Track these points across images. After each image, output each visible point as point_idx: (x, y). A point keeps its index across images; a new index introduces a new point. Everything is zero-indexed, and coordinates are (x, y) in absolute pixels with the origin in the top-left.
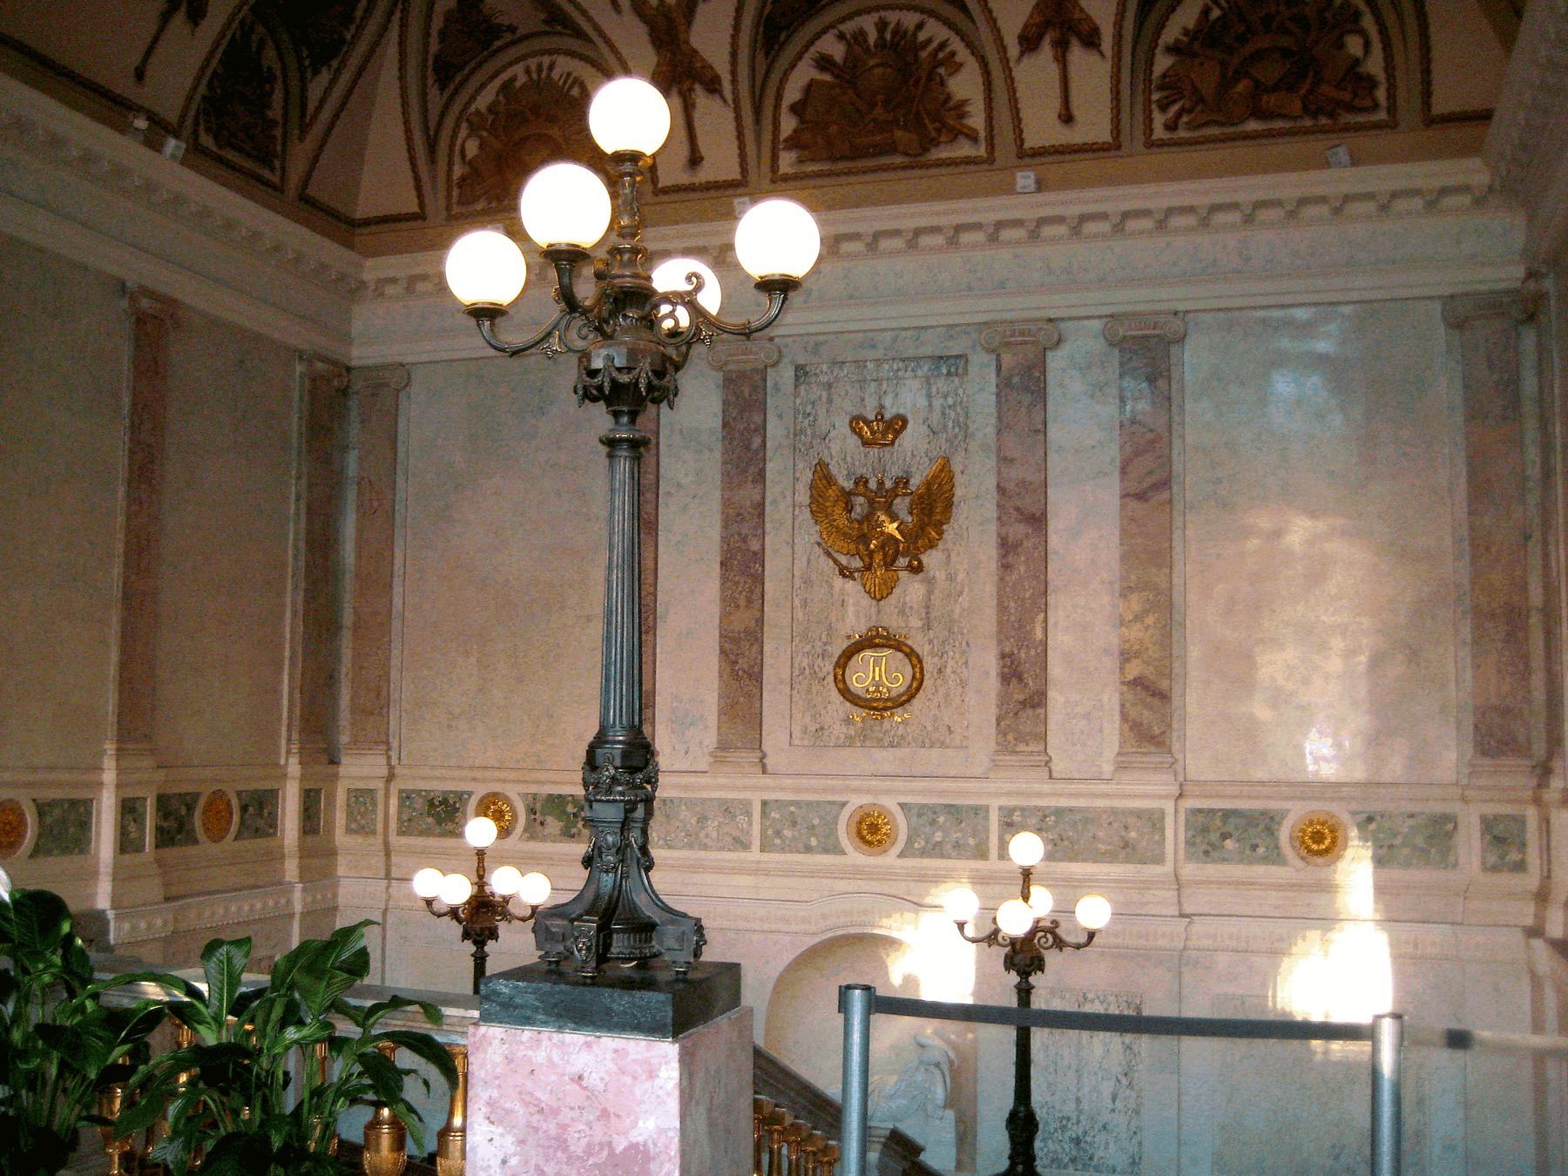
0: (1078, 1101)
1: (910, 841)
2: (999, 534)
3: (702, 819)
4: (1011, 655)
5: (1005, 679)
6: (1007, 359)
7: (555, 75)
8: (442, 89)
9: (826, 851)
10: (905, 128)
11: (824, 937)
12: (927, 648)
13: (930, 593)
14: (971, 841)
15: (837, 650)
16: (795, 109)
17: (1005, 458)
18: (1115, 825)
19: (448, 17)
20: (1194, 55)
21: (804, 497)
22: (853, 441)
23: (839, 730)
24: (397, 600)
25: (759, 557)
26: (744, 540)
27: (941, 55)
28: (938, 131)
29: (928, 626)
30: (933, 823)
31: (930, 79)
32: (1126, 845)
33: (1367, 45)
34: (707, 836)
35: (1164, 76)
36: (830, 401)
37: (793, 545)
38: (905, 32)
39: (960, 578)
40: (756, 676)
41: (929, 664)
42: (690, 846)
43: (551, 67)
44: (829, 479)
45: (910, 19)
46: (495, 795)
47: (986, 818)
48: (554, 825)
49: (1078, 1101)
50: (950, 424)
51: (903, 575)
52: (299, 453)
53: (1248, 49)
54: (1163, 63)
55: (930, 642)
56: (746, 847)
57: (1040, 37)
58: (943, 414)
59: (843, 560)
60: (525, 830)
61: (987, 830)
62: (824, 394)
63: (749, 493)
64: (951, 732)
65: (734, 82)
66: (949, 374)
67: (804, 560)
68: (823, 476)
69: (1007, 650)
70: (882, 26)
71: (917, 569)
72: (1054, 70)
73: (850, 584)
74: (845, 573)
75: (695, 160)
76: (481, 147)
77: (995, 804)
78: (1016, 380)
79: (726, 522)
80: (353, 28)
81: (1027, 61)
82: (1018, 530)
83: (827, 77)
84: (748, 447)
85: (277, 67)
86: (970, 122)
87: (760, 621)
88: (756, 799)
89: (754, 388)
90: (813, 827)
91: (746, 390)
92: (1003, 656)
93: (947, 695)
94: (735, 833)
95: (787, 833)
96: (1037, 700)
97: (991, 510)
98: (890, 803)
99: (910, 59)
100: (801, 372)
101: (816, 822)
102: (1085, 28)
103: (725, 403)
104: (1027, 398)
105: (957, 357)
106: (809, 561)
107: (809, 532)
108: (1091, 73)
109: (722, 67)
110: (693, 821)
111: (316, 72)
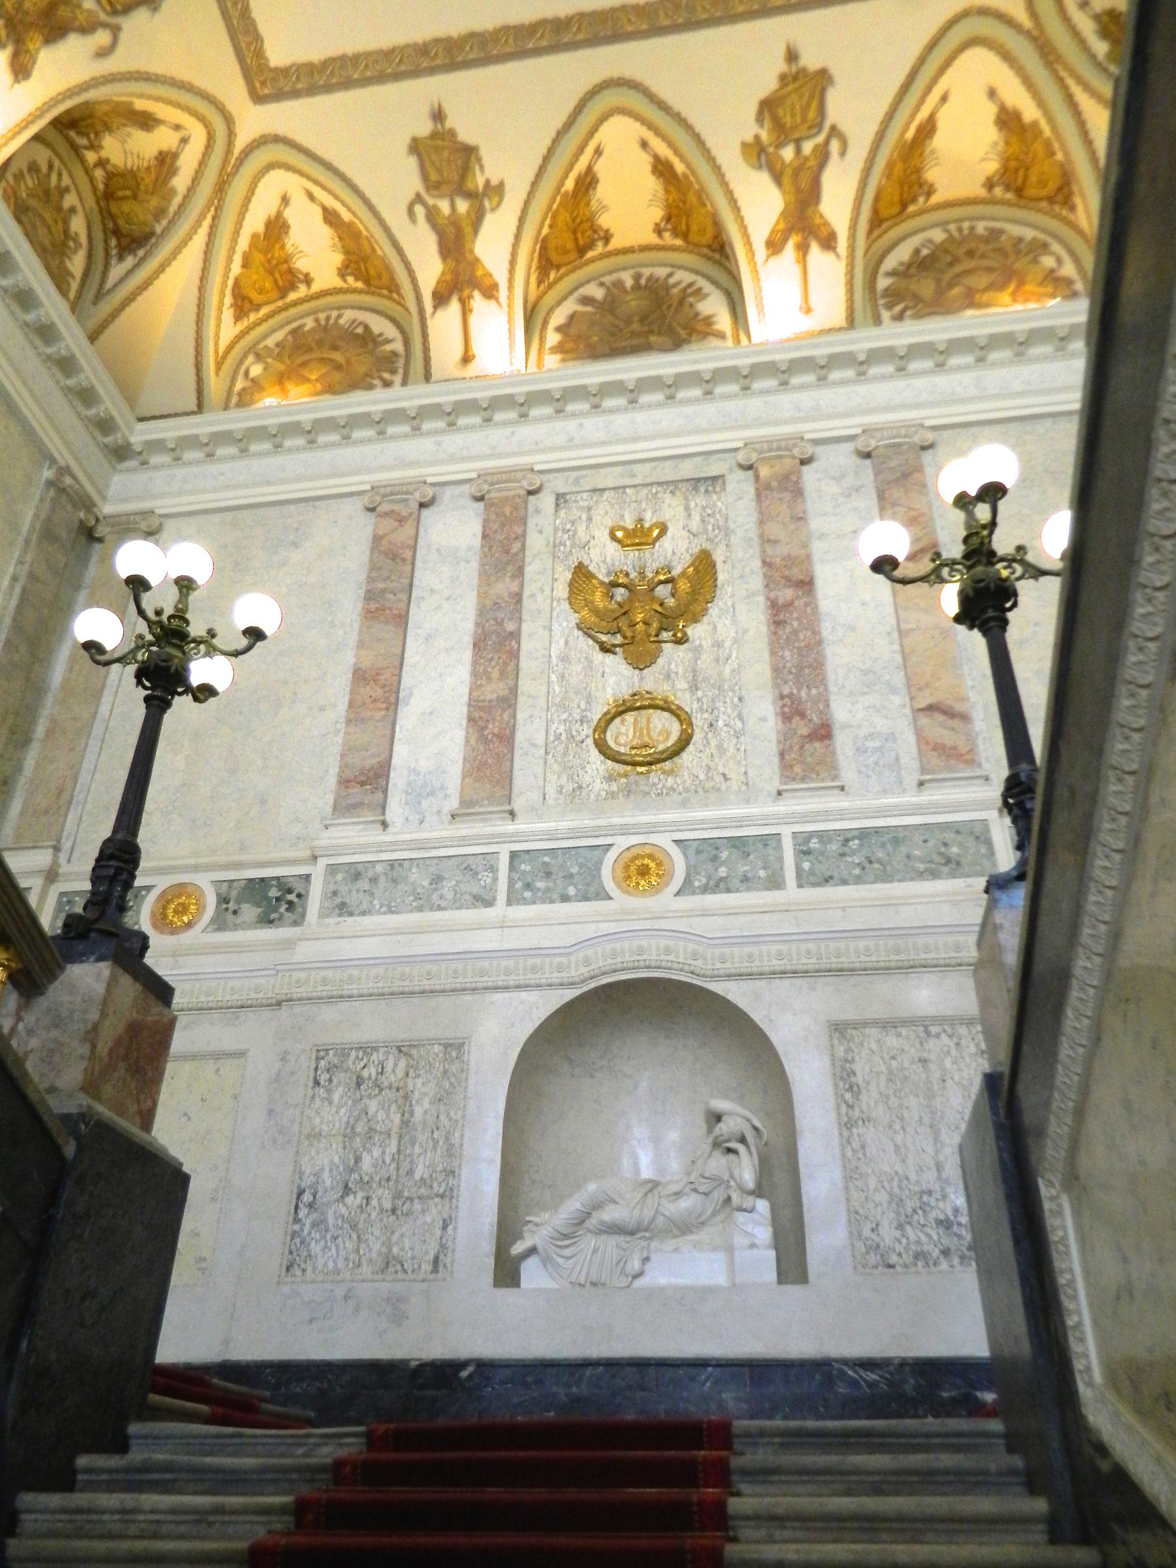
0: (939, 1167)
1: (688, 881)
2: (768, 598)
3: (437, 879)
4: (790, 696)
5: (786, 718)
6: (764, 472)
7: (342, 321)
8: (237, 318)
9: (586, 898)
10: (660, 333)
11: (586, 989)
12: (695, 705)
13: (696, 659)
14: (762, 873)
15: (596, 715)
16: (559, 329)
17: (769, 541)
18: (931, 844)
19: (255, 236)
20: (911, 276)
21: (562, 591)
22: (612, 548)
23: (599, 786)
24: (104, 709)
25: (516, 635)
26: (501, 624)
27: (689, 291)
28: (690, 334)
29: (694, 687)
30: (715, 859)
31: (681, 303)
32: (948, 861)
33: (1059, 261)
34: (441, 897)
35: (887, 289)
36: (590, 519)
37: (551, 631)
38: (657, 280)
39: (727, 644)
40: (507, 738)
41: (699, 721)
42: (420, 909)
43: (339, 316)
44: (590, 576)
45: (661, 272)
46: (182, 885)
47: (779, 847)
48: (249, 912)
49: (939, 1167)
50: (710, 528)
51: (668, 647)
52: (27, 541)
53: (957, 269)
54: (883, 283)
55: (699, 700)
56: (489, 903)
57: (785, 240)
58: (703, 521)
59: (604, 638)
60: (213, 921)
61: (781, 859)
62: (584, 516)
63: (504, 587)
64: (726, 779)
65: (511, 287)
66: (707, 491)
67: (562, 642)
68: (581, 573)
69: (786, 691)
70: (637, 277)
71: (679, 642)
72: (797, 269)
73: (609, 659)
74: (606, 649)
75: (467, 359)
76: (265, 369)
77: (786, 832)
78: (774, 484)
79: (481, 613)
80: (164, 223)
81: (775, 261)
82: (788, 594)
83: (589, 309)
84: (507, 552)
85: (83, 239)
86: (717, 327)
87: (514, 690)
88: (504, 852)
89: (516, 508)
90: (571, 876)
91: (507, 510)
92: (782, 697)
93: (720, 747)
94: (475, 890)
95: (540, 884)
96: (823, 732)
97: (756, 583)
98: (664, 841)
99: (663, 293)
100: (561, 499)
101: (575, 870)
102: (824, 232)
103: (486, 523)
104: (787, 496)
105: (715, 479)
106: (567, 643)
107: (566, 620)
108: (829, 272)
109: (500, 275)
110: (426, 883)
111: (121, 258)
